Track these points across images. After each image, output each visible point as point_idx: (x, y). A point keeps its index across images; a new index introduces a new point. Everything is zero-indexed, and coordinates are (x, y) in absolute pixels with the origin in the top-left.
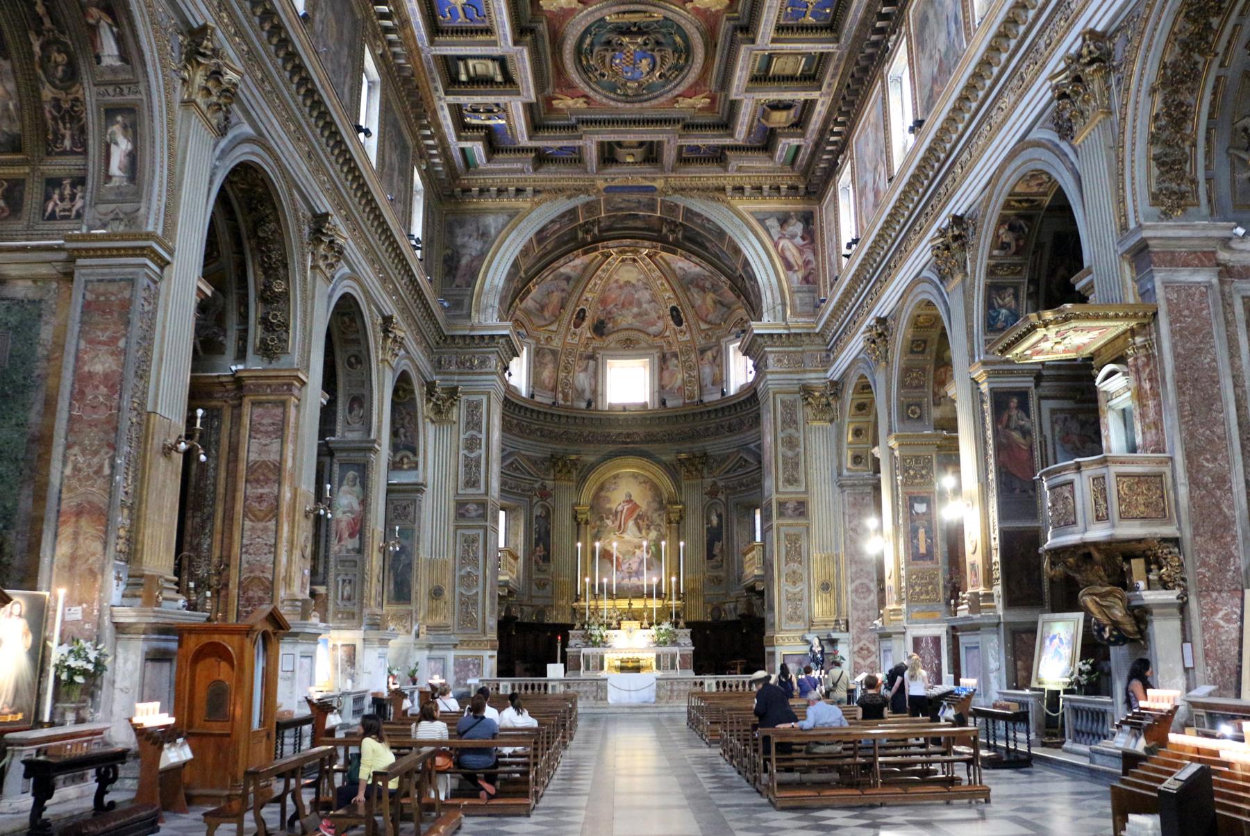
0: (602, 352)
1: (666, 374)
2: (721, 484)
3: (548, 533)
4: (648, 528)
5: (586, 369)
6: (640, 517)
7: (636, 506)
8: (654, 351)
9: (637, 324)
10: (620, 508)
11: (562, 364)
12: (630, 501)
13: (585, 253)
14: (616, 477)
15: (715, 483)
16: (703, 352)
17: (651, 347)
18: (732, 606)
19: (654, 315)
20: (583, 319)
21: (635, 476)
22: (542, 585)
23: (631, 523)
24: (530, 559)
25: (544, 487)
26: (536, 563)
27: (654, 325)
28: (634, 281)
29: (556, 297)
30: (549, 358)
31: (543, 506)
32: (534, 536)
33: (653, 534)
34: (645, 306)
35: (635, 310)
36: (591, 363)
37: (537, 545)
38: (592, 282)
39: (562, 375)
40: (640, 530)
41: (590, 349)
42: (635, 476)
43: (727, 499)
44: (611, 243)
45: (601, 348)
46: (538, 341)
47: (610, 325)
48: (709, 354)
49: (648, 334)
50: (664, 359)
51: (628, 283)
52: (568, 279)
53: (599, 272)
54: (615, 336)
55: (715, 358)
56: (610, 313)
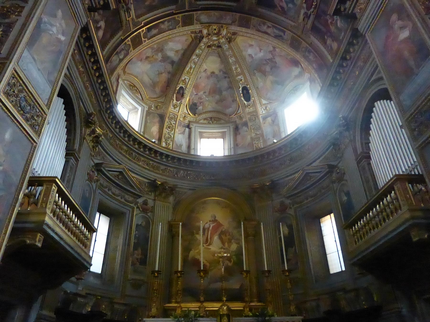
0: (195, 125)
1: (239, 138)
2: (288, 202)
3: (146, 239)
4: (230, 242)
5: (183, 133)
6: (222, 233)
7: (219, 225)
8: (230, 125)
9: (219, 108)
10: (207, 226)
11: (166, 124)
12: (215, 220)
13: (185, 24)
14: (205, 203)
15: (282, 203)
16: (265, 118)
17: (227, 122)
18: (314, 304)
19: (230, 99)
20: (183, 96)
21: (218, 203)
22: (136, 285)
23: (216, 238)
24: (127, 259)
25: (145, 203)
26: (133, 264)
27: (230, 107)
28: (217, 72)
29: (165, 77)
30: (157, 119)
31: (143, 217)
32: (133, 241)
33: (234, 247)
34: (224, 93)
35: (217, 97)
36: (187, 130)
37: (135, 248)
38: (189, 66)
39: (165, 131)
40: (223, 243)
41: (187, 122)
42: (218, 203)
43: (295, 212)
44: (204, 17)
45: (196, 122)
46: (150, 108)
47: (200, 108)
48: (269, 119)
49: (225, 115)
50: (236, 129)
51: (213, 73)
52: (172, 63)
53: (194, 57)
54: (204, 116)
55: (273, 121)
56: (200, 98)
